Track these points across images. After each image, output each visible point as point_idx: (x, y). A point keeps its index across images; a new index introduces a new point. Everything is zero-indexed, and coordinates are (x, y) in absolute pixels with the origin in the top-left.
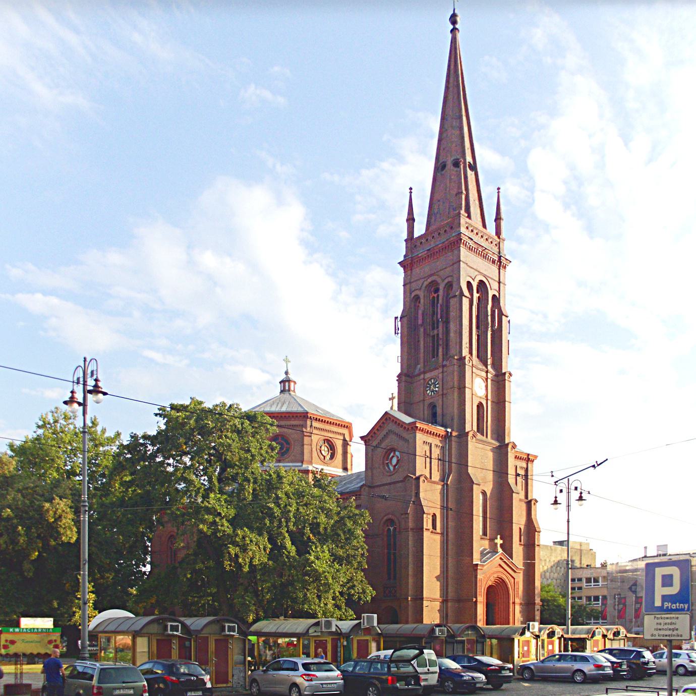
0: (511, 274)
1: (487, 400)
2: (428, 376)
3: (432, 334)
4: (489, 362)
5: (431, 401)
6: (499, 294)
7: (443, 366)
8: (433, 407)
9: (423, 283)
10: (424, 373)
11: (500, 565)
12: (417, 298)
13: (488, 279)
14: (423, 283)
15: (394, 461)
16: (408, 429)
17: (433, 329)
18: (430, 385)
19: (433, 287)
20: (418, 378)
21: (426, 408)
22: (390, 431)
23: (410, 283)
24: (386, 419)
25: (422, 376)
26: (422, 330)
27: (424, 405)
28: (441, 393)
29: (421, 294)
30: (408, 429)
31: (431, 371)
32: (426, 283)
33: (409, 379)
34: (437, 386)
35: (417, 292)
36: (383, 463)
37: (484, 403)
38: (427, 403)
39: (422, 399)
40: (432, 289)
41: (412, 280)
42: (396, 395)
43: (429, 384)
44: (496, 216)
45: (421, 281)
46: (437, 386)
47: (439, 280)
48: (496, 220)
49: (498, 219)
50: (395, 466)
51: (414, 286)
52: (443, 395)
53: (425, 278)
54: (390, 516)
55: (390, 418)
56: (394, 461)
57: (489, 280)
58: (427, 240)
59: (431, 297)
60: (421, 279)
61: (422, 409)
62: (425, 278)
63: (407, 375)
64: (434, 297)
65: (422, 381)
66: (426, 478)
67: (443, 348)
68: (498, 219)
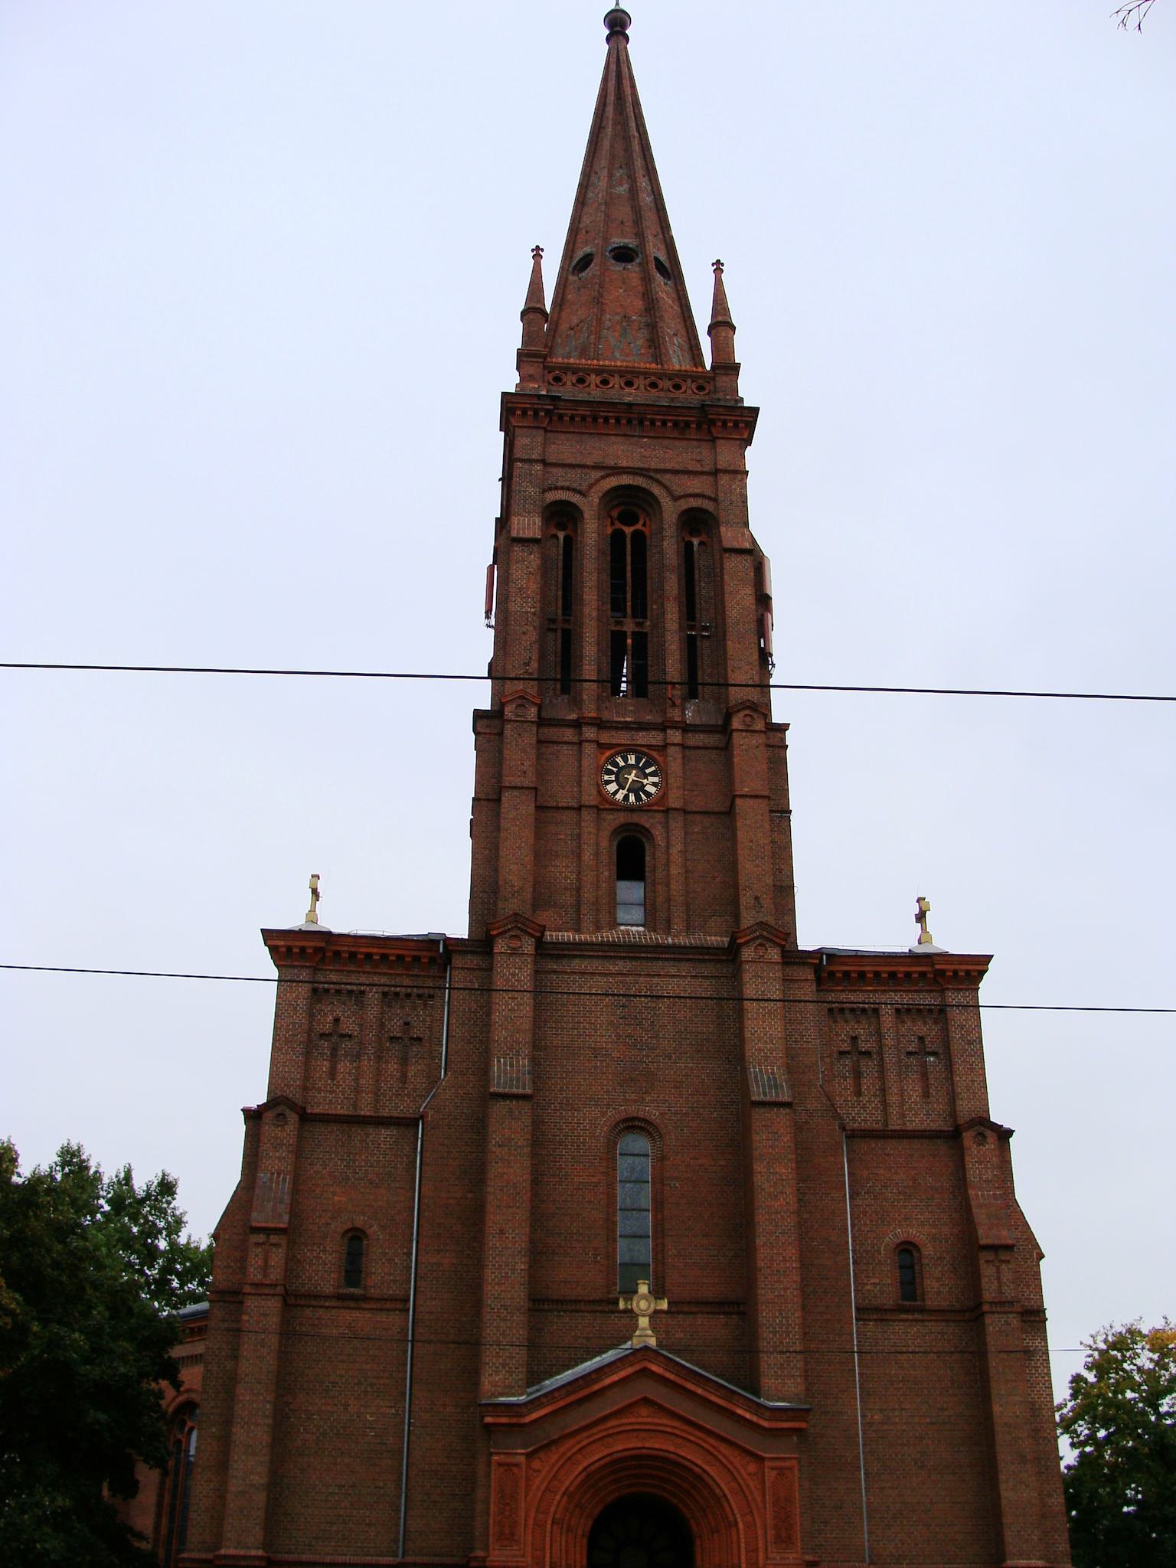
5: (635, 818)
7: (686, 729)
9: (598, 481)
14: (598, 481)
19: (630, 503)
20: (569, 734)
21: (606, 834)
29: (590, 507)
31: (626, 727)
35: (575, 499)
40: (615, 514)
43: (616, 765)
45: (595, 475)
47: (656, 490)
51: (560, 476)
58: (605, 382)
59: (609, 531)
62: (603, 468)
64: (617, 538)
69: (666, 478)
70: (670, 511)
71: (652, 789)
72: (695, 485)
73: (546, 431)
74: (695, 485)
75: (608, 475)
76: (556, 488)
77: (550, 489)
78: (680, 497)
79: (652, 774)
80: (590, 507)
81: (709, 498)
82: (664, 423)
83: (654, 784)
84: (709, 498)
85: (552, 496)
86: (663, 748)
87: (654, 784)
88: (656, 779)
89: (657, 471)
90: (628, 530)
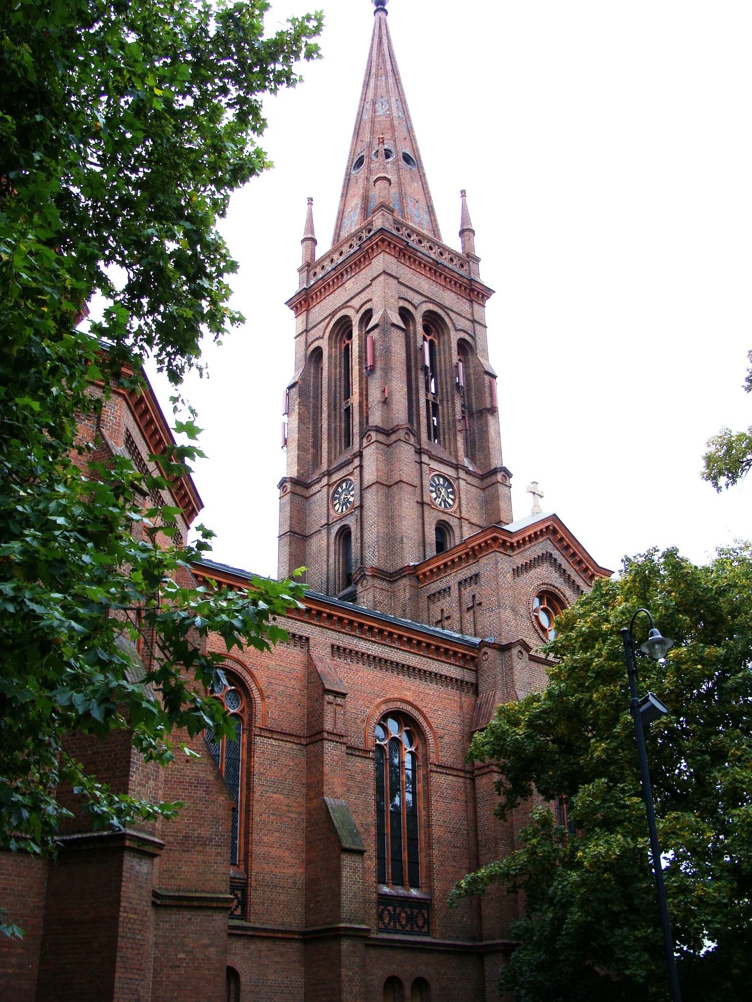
0: (492, 311)
2: (336, 477)
6: (474, 339)
8: (345, 534)
10: (329, 474)
12: (317, 353)
13: (449, 312)
18: (340, 494)
19: (343, 328)
23: (307, 331)
25: (325, 481)
27: (329, 533)
28: (357, 504)
29: (324, 344)
33: (299, 490)
34: (352, 493)
37: (453, 522)
38: (335, 529)
39: (324, 521)
41: (310, 326)
43: (338, 493)
44: (462, 224)
45: (324, 324)
46: (352, 493)
48: (462, 233)
49: (466, 232)
53: (330, 315)
57: (451, 314)
61: (325, 542)
63: (295, 482)
65: (325, 489)
68: (466, 232)
70: (356, 319)
71: (351, 499)
72: (363, 297)
74: (363, 297)
75: (331, 319)
76: (312, 342)
79: (352, 490)
80: (324, 344)
82: (351, 267)
83: (352, 496)
86: (351, 474)
87: (352, 496)
89: (347, 302)
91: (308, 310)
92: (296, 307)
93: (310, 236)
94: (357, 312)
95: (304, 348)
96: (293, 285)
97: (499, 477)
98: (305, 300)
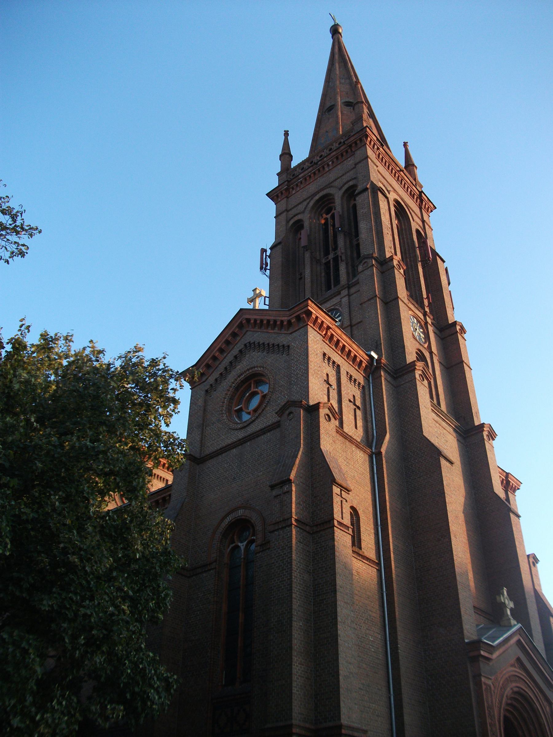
1: (431, 353)
3: (324, 261)
4: (426, 302)
9: (308, 203)
11: (518, 660)
12: (298, 226)
14: (308, 203)
15: (255, 402)
16: (289, 322)
17: (327, 253)
19: (324, 204)
22: (250, 346)
23: (287, 211)
24: (241, 326)
26: (307, 255)
30: (289, 322)
32: (311, 204)
36: (229, 410)
42: (265, 292)
50: (255, 410)
52: (351, 326)
54: (240, 512)
55: (248, 320)
56: (255, 402)
60: (305, 200)
66: (331, 409)
67: (347, 264)
69: (336, 184)
70: (338, 196)
73: (287, 197)
75: (312, 199)
77: (290, 220)
78: (341, 187)
81: (353, 179)
84: (353, 179)
85: (291, 222)
88: (340, 318)
90: (329, 216)
91: (287, 197)
92: (277, 196)
93: (287, 151)
94: (340, 189)
95: (284, 223)
96: (274, 183)
97: (458, 328)
98: (287, 190)
